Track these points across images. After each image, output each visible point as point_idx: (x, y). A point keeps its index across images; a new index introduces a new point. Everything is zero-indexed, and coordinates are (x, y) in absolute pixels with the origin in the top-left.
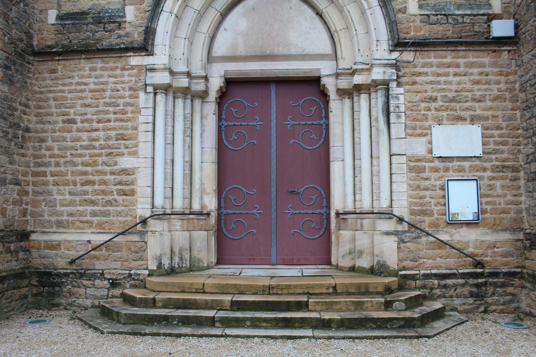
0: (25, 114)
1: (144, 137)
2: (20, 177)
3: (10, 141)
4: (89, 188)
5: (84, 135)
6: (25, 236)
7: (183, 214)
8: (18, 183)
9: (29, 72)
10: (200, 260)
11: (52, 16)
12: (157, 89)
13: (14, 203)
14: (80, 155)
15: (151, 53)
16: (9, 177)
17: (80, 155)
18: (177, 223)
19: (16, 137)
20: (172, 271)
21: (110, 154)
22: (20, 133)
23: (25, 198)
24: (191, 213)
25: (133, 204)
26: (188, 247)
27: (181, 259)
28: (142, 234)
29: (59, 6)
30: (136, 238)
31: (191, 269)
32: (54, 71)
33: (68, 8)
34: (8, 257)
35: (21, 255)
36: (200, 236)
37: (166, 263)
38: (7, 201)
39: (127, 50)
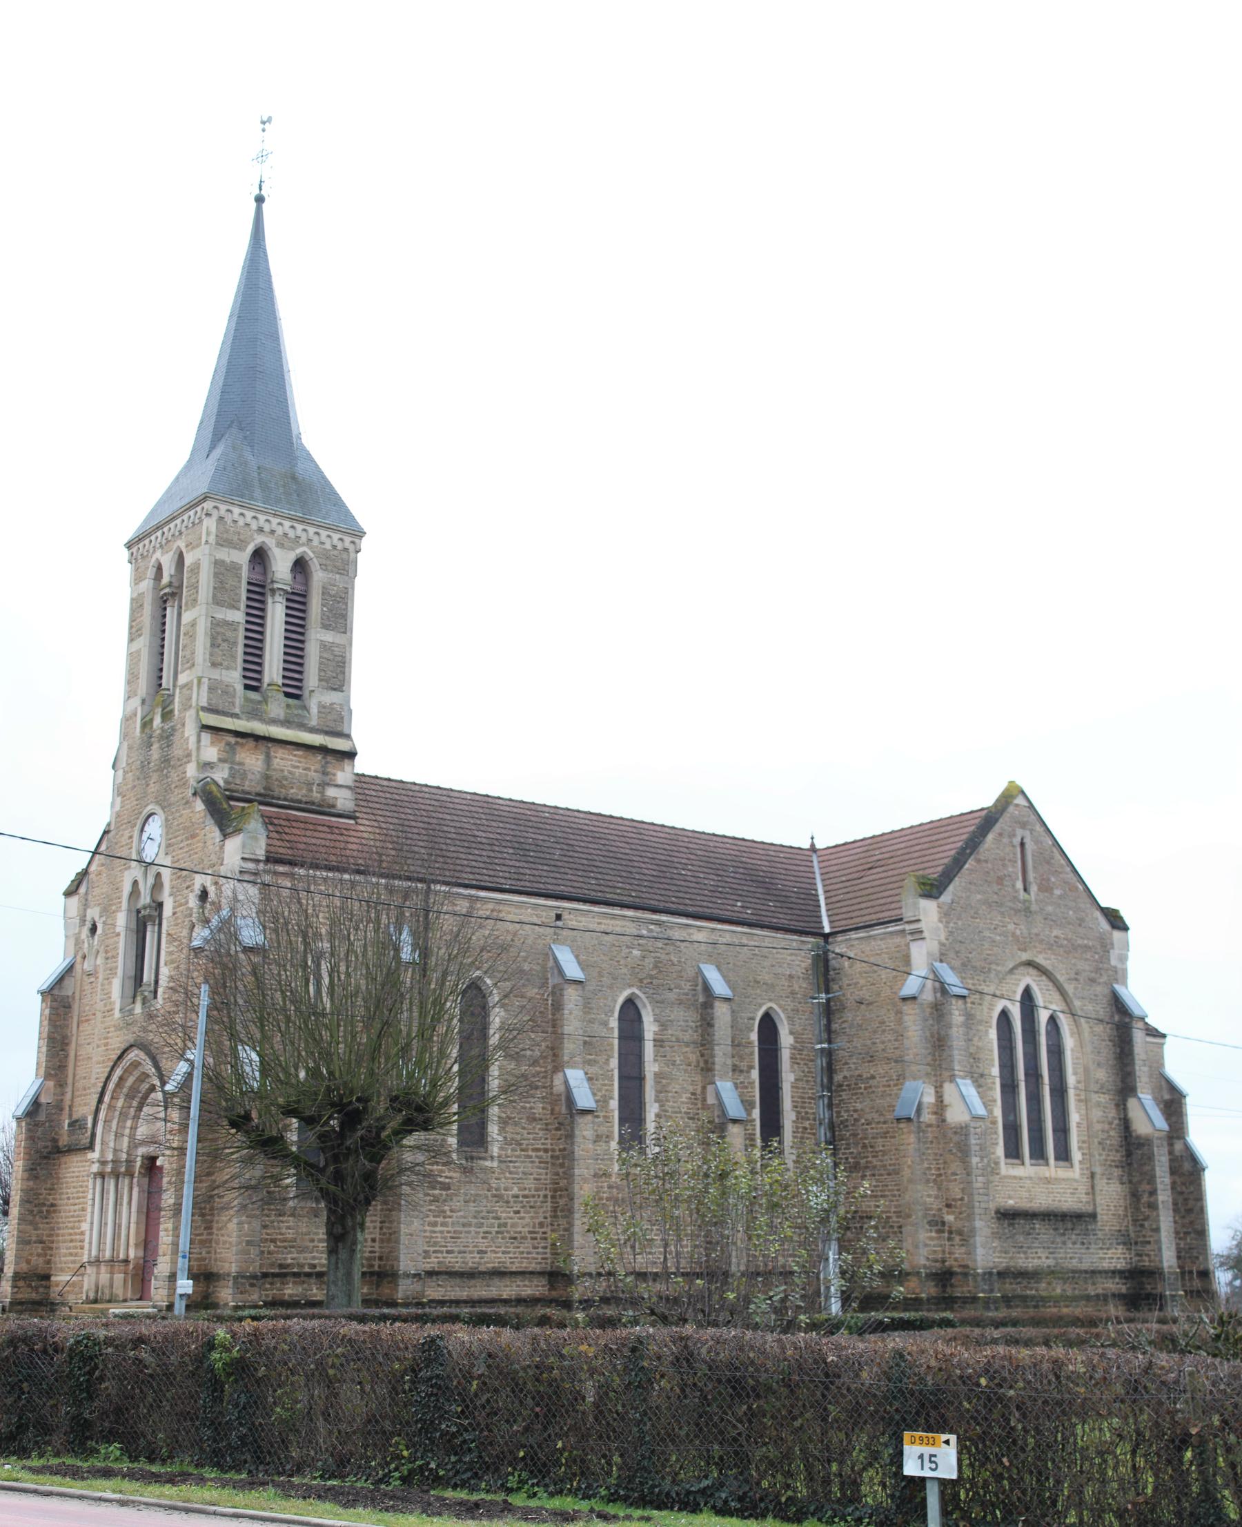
0: (50, 1195)
1: (89, 1209)
2: (45, 1238)
3: (34, 1216)
4: (71, 1244)
5: (72, 1208)
6: (47, 1277)
7: (113, 1261)
8: (41, 1242)
9: (54, 1165)
10: (117, 1295)
11: (67, 1122)
12: (95, 1175)
13: (39, 1255)
14: (70, 1222)
15: (94, 1151)
16: (34, 1239)
17: (70, 1222)
18: (103, 1268)
19: (41, 1212)
20: (96, 1301)
21: (79, 1221)
22: (45, 1209)
23: (49, 1252)
24: (119, 1261)
25: (82, 1255)
26: (108, 1284)
27: (103, 1293)
28: (83, 1275)
29: (70, 1116)
30: (80, 1278)
31: (109, 1301)
32: (66, 1163)
33: (75, 1117)
34: (29, 1290)
35: (41, 1290)
36: (119, 1278)
37: (92, 1296)
38: (31, 1254)
39: (85, 1149)
